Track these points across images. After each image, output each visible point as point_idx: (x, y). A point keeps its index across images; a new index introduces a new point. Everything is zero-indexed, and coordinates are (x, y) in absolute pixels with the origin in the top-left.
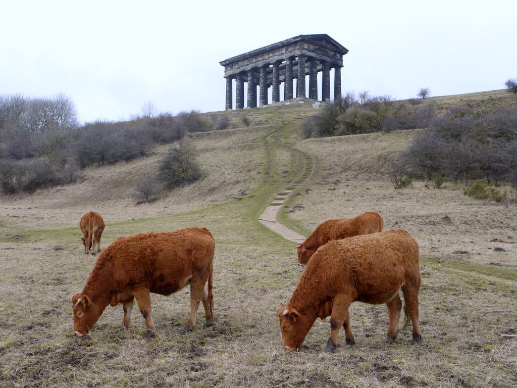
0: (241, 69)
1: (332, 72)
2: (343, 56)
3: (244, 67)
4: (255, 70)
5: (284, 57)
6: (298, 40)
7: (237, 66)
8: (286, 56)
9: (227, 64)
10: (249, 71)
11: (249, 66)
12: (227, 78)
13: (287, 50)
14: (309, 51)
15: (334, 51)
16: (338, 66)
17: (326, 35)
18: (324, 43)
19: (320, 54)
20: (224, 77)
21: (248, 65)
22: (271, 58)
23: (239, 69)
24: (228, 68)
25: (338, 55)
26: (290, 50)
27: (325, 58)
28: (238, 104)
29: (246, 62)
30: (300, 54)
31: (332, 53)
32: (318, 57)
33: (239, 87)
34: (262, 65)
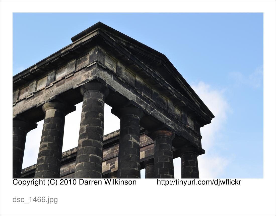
8: (47, 96)
15: (182, 108)
17: (164, 56)
19: (148, 101)
25: (190, 123)
26: (59, 77)
27: (161, 116)
31: (177, 112)
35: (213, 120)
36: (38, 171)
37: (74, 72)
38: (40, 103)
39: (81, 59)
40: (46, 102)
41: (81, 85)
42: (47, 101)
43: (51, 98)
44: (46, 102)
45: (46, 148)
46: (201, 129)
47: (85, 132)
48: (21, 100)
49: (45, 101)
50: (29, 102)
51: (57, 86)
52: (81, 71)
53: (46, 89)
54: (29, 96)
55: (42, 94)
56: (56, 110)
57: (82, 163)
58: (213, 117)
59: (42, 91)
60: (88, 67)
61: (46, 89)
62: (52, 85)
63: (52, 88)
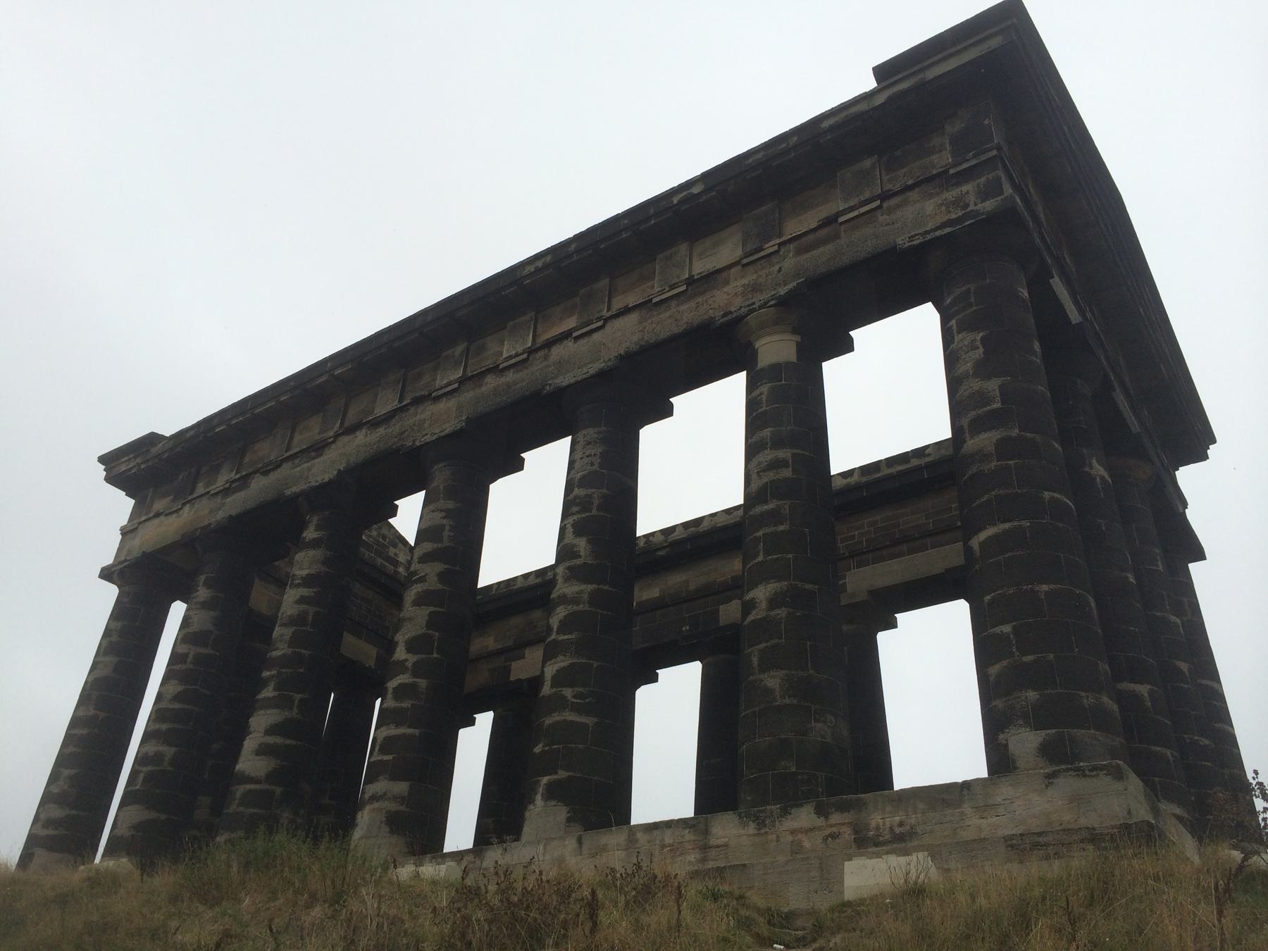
0: (260, 488)
3: (286, 470)
10: (320, 496)
11: (331, 454)
20: (106, 574)
21: (318, 448)
22: (557, 352)
23: (241, 495)
29: (311, 431)
33: (193, 651)
36: (767, 553)
37: (885, 196)
38: (725, 315)
39: (898, 153)
40: (761, 307)
41: (938, 233)
42: (766, 303)
43: (783, 291)
44: (761, 307)
45: (787, 473)
47: (997, 405)
48: (626, 311)
49: (754, 303)
50: (668, 314)
51: (799, 252)
52: (917, 190)
53: (744, 266)
54: (662, 292)
55: (727, 283)
56: (798, 338)
57: (1016, 523)
59: (724, 274)
60: (952, 171)
61: (744, 266)
62: (776, 248)
63: (774, 259)
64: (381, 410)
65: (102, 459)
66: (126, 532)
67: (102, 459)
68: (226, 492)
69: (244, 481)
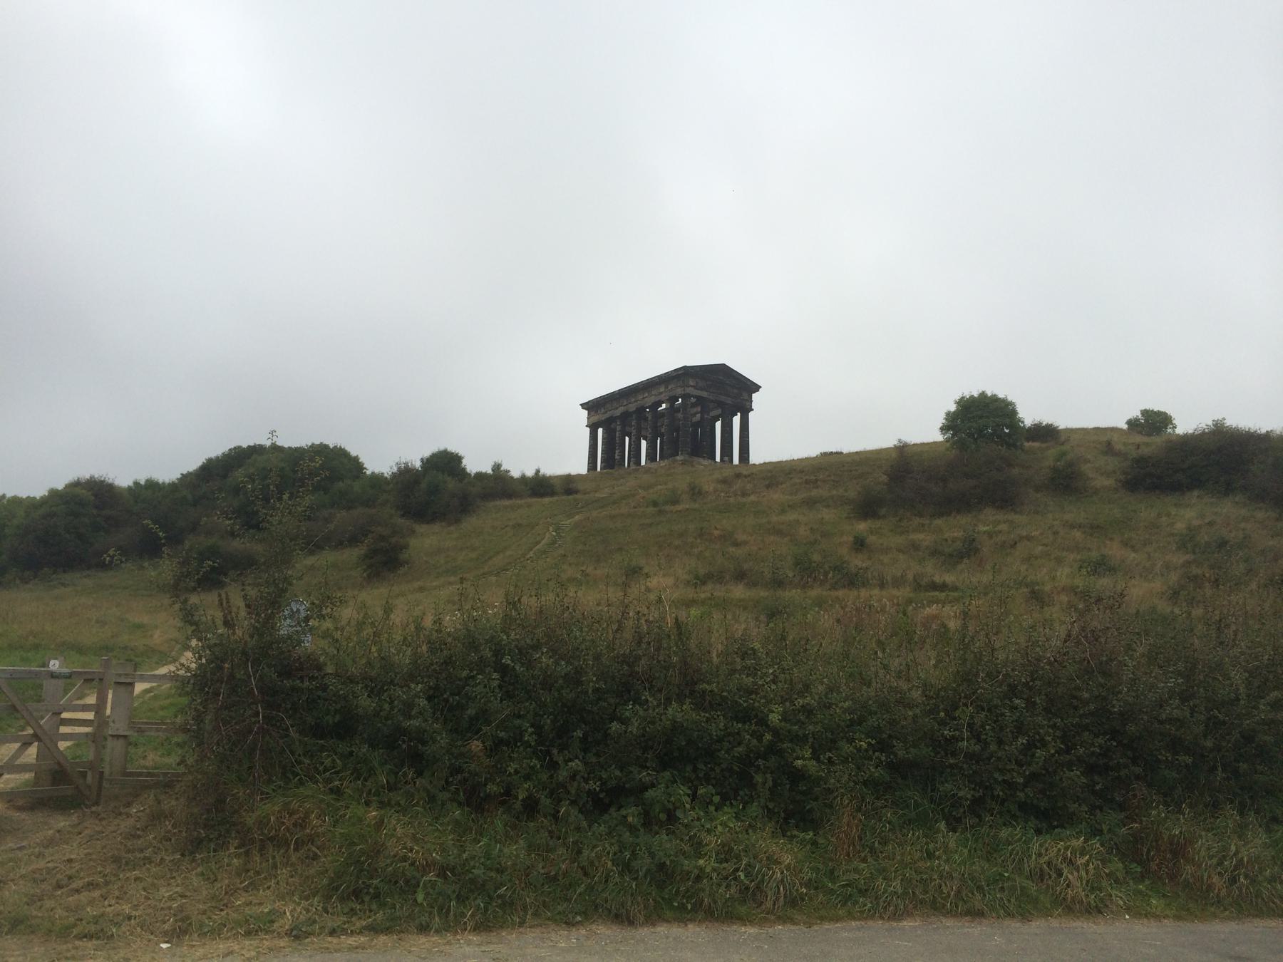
0: (608, 415)
1: (736, 420)
2: (753, 395)
4: (625, 416)
5: (663, 397)
6: (680, 373)
7: (603, 411)
8: (665, 396)
9: (591, 406)
12: (590, 427)
13: (666, 387)
14: (698, 389)
16: (745, 410)
17: (724, 365)
18: (721, 378)
20: (587, 426)
21: (617, 408)
24: (592, 413)
26: (670, 388)
27: (723, 398)
28: (603, 464)
30: (683, 393)
31: (735, 391)
32: (711, 397)
34: (634, 409)
35: (760, 390)
46: (753, 395)
58: (760, 387)
64: (625, 404)
65: (584, 406)
66: (588, 418)
67: (584, 406)
68: (604, 413)
69: (606, 412)
